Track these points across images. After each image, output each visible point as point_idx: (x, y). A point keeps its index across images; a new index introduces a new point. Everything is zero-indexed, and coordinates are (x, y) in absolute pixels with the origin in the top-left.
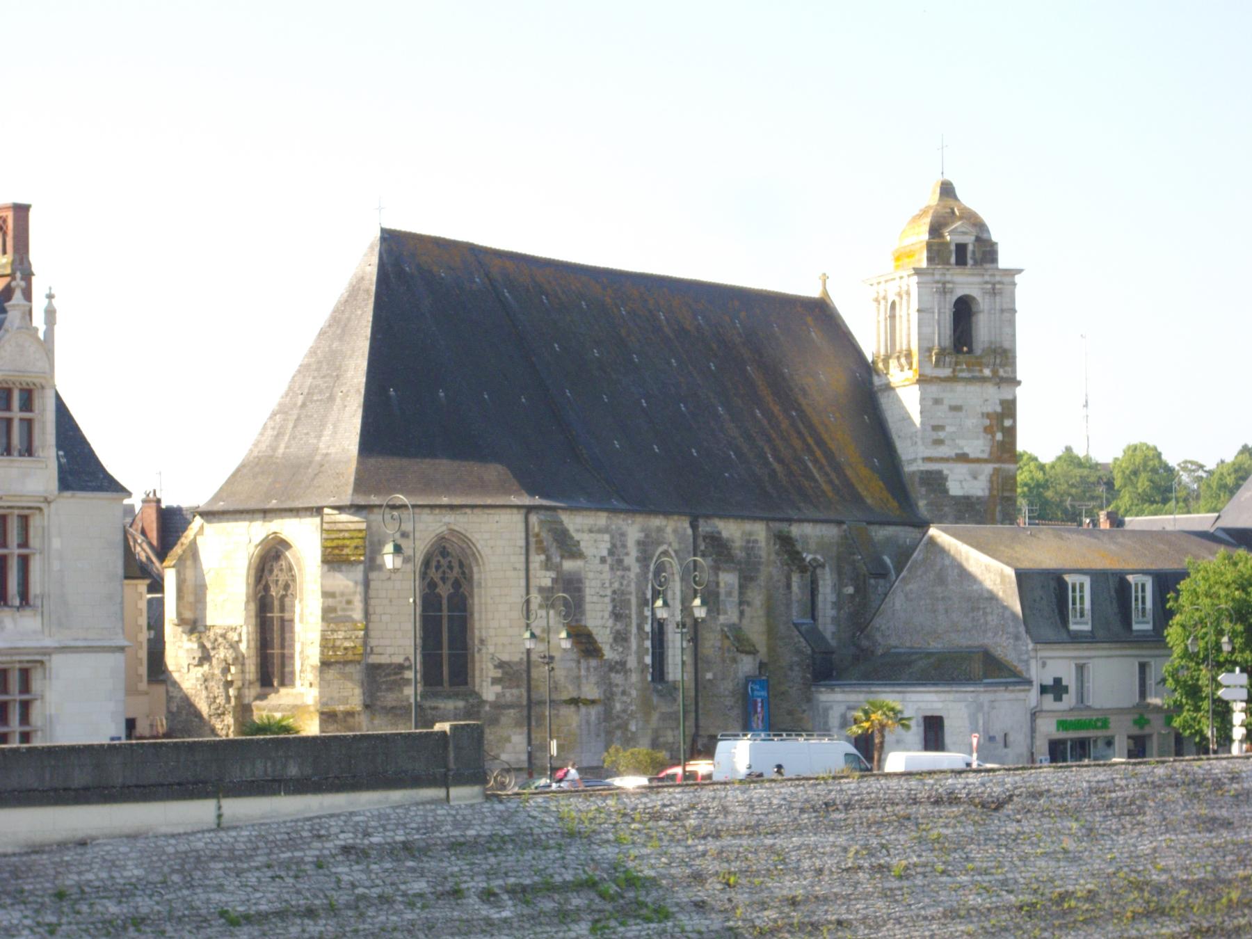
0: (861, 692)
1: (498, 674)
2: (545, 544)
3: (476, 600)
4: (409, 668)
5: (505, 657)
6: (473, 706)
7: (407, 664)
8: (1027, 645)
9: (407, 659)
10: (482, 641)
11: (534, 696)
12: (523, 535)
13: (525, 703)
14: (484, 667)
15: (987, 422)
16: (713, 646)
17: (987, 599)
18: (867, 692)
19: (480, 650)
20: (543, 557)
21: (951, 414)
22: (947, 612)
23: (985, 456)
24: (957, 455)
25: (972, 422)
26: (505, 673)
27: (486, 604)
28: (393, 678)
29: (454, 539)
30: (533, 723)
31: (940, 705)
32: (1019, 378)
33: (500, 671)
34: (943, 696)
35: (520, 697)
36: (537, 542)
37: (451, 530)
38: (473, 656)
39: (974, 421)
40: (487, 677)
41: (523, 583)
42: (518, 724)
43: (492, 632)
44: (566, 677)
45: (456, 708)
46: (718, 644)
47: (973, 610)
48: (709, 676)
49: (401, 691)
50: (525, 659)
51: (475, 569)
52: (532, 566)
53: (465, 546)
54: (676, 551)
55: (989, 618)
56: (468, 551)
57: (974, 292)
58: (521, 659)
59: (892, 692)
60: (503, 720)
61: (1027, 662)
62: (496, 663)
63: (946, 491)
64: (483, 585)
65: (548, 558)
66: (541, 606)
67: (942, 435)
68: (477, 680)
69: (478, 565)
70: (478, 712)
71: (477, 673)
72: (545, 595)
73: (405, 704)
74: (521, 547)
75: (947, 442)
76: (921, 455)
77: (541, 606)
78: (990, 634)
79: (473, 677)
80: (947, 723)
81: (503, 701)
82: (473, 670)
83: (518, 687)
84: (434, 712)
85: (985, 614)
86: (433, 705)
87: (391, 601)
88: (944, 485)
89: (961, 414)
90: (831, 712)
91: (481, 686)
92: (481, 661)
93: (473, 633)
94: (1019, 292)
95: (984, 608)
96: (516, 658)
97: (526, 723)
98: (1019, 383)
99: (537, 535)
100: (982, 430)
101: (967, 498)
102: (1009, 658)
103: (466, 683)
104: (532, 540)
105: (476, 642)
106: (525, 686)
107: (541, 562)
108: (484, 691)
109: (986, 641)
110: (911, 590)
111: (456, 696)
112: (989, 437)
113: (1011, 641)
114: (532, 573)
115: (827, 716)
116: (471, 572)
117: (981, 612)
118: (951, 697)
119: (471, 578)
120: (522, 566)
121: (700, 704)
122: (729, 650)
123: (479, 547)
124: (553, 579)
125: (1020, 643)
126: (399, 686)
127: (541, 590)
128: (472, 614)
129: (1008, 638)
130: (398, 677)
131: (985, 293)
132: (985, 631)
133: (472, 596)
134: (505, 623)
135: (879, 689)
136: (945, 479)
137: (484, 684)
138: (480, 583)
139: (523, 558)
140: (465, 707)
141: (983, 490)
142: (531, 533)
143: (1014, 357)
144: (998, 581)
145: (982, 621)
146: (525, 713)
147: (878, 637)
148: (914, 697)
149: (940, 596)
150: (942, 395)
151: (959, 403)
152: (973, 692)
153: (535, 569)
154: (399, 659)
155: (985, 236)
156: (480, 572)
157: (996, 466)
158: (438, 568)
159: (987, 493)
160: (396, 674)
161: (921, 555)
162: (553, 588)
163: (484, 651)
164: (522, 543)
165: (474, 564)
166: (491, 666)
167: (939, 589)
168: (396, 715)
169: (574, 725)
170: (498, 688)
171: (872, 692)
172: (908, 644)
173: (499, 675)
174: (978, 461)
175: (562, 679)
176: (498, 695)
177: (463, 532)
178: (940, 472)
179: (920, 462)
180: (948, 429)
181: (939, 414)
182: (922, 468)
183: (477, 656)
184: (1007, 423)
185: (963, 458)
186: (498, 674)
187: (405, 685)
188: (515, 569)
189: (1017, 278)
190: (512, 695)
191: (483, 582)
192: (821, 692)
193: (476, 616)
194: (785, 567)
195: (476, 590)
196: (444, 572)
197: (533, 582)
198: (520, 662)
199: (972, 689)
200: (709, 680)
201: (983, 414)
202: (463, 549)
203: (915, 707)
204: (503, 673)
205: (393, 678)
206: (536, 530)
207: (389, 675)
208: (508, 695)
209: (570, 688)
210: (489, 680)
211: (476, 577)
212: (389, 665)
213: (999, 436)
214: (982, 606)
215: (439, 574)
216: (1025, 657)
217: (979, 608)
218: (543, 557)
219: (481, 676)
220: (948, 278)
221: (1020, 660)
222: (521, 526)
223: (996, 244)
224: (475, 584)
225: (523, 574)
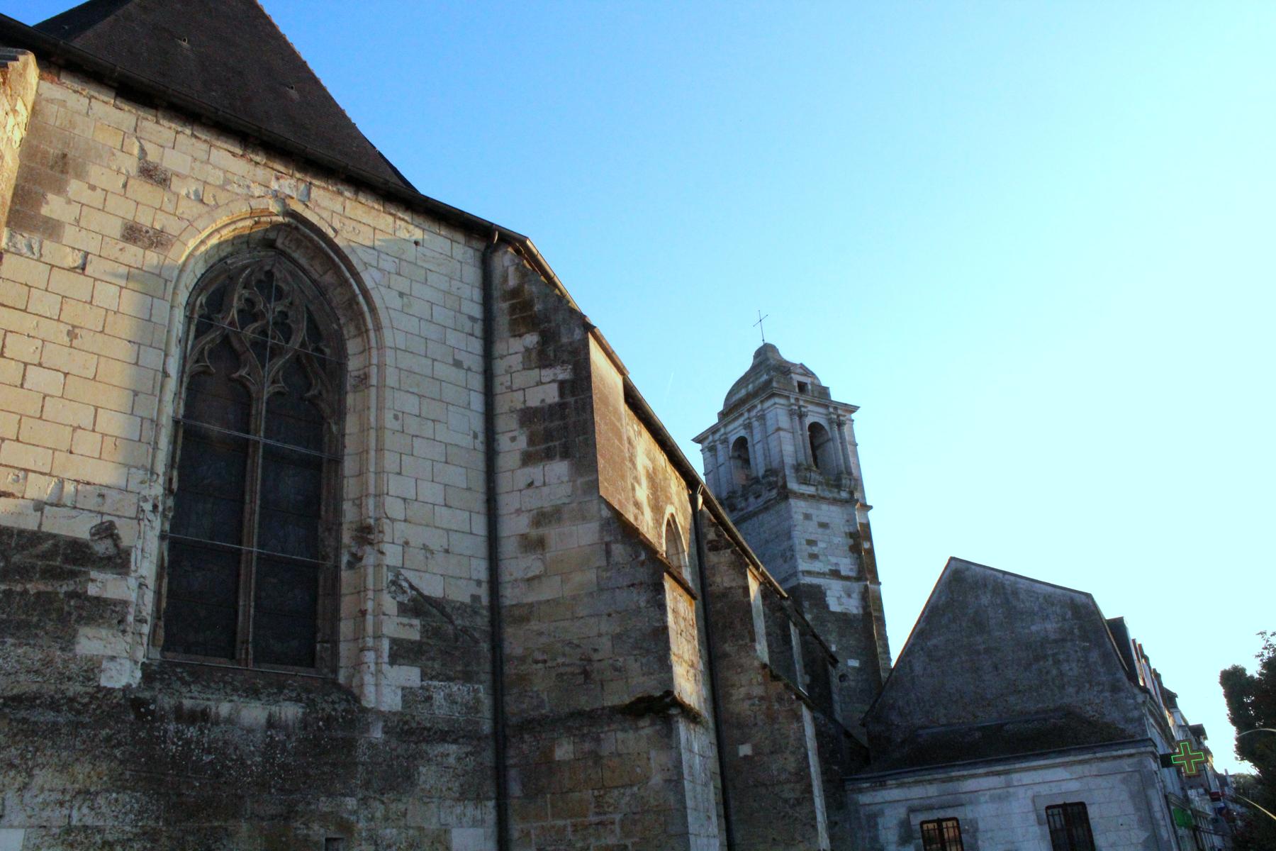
0: (930, 782)
1: (412, 631)
2: (538, 307)
3: (351, 424)
4: (119, 562)
5: (432, 587)
6: (329, 720)
7: (102, 547)
8: (1134, 697)
9: (107, 531)
10: (365, 534)
11: (515, 706)
12: (477, 294)
13: (487, 727)
14: (370, 606)
15: (851, 542)
16: (749, 697)
17: (1056, 641)
18: (943, 781)
19: (356, 560)
20: (531, 339)
21: (820, 530)
22: (996, 668)
23: (853, 574)
24: (830, 570)
25: (841, 541)
26: (431, 632)
27: (380, 429)
28: (32, 588)
29: (296, 255)
30: (515, 789)
31: (1074, 786)
32: (869, 503)
33: (416, 622)
34: (1079, 769)
35: (474, 708)
36: (513, 309)
37: (293, 215)
38: (336, 579)
39: (840, 539)
40: (378, 637)
41: (477, 402)
42: (468, 794)
43: (394, 508)
44: (616, 638)
45: (271, 723)
46: (758, 691)
47: (1037, 659)
48: (745, 750)
49: (68, 643)
50: (485, 601)
51: (352, 346)
52: (500, 366)
53: (329, 278)
54: (682, 526)
55: (1065, 667)
56: (337, 297)
57: (823, 422)
58: (475, 598)
59: (987, 774)
60: (427, 775)
61: (1140, 720)
62: (405, 599)
63: (827, 607)
64: (374, 381)
65: (548, 338)
66: (528, 459)
67: (815, 550)
68: (344, 648)
69: (362, 331)
70: (350, 745)
71: (346, 628)
72: (539, 427)
73: (74, 688)
74: (472, 318)
75: (820, 557)
77: (528, 459)
78: (1071, 690)
79: (335, 643)
80: (1093, 812)
81: (422, 714)
82: (335, 618)
83: (468, 677)
84: (192, 732)
85: (1057, 662)
86: (187, 703)
87: (72, 334)
88: (825, 601)
90: (880, 821)
91: (358, 665)
92: (360, 591)
93: (338, 512)
94: (856, 426)
95: (1054, 655)
96: (461, 593)
97: (489, 788)
98: (871, 507)
99: (515, 293)
100: (847, 548)
101: (845, 614)
102: (1108, 719)
103: (309, 659)
104: (501, 307)
105: (346, 538)
106: (487, 677)
107: (528, 350)
108: (369, 679)
109: (1067, 700)
110: (936, 646)
111: (278, 689)
113: (1107, 694)
114: (501, 381)
115: (876, 824)
116: (342, 353)
117: (1050, 662)
118: (1094, 768)
119: (341, 366)
120: (476, 363)
121: (733, 803)
122: (780, 699)
123: (369, 284)
124: (562, 384)
125: (1122, 694)
126: (63, 619)
127: (528, 416)
128: (337, 461)
129: (1102, 691)
130: (65, 587)
131: (831, 422)
132: (1062, 687)
133: (340, 414)
134: (431, 492)
135: (965, 773)
136: (825, 594)
137: (370, 657)
138: (364, 379)
139: (477, 346)
140: (305, 724)
141: (857, 608)
142: (496, 294)
143: (862, 485)
144: (1069, 614)
145: (1054, 672)
146: (488, 757)
147: (895, 718)
148: (1027, 778)
149: (982, 647)
150: (810, 511)
151: (825, 520)
152: (1131, 756)
153: (509, 371)
154: (80, 528)
155: (816, 382)
156: (366, 350)
158: (249, 314)
159: (861, 611)
160: (52, 574)
161: (943, 598)
162: (562, 406)
163: (370, 558)
164: (477, 311)
165: (349, 331)
166: (389, 604)
167: (979, 639)
168: (29, 731)
169: (657, 779)
170: (410, 675)
171: (951, 780)
172: (943, 721)
173: (415, 636)
174: (847, 578)
175: (606, 644)
176: (407, 693)
177: (331, 233)
178: (819, 587)
180: (822, 545)
181: (810, 530)
183: (345, 575)
184: (866, 545)
185: (835, 574)
186: (412, 631)
187: (90, 620)
188: (458, 364)
189: (853, 416)
190: (450, 698)
191: (374, 370)
192: (861, 791)
193: (349, 466)
194: (778, 614)
195: (350, 399)
196: (264, 333)
197: (504, 403)
198: (471, 609)
199: (1133, 751)
200: (746, 757)
201: (846, 533)
202: (322, 291)
203: (1030, 793)
204: (424, 631)
205: (32, 588)
206: (512, 282)
207: (24, 573)
208: (439, 697)
209: (633, 666)
210: (386, 645)
211: (353, 364)
212: (36, 537)
214: (1050, 652)
215: (250, 331)
216: (1136, 714)
217: (1045, 657)
218: (531, 339)
219: (359, 635)
220: (801, 403)
221: (1131, 720)
222: (472, 273)
223: (828, 388)
224: (350, 382)
225: (477, 382)
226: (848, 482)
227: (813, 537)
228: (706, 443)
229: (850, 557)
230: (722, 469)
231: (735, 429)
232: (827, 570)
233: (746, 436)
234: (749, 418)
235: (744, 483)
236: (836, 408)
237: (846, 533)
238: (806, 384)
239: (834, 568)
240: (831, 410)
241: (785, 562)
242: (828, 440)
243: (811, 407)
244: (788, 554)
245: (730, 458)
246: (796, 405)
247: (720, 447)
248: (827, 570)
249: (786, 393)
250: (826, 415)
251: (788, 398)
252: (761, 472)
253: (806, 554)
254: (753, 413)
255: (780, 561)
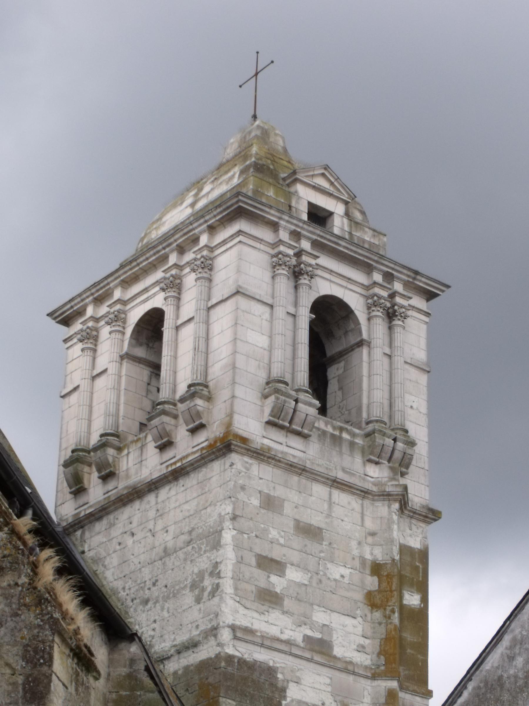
21: (297, 542)
23: (360, 658)
24: (307, 639)
39: (346, 572)
75: (287, 603)
76: (229, 620)
89: (313, 547)
100: (359, 596)
112: (378, 615)
150: (279, 492)
157: (394, 684)
178: (271, 671)
179: (226, 635)
181: (273, 533)
182: (230, 651)
213: (396, 618)
220: (306, 245)
226: (389, 442)
227: (276, 554)
228: (77, 326)
229: (364, 617)
230: (100, 382)
231: (146, 290)
232: (298, 637)
233: (164, 308)
234: (176, 265)
235: (147, 417)
236: (389, 277)
237: (363, 561)
238: (331, 214)
239: (318, 635)
240: (378, 277)
241: (198, 600)
242: (360, 344)
243: (325, 261)
244: (208, 583)
245: (122, 357)
246: (290, 247)
247: (105, 331)
248: (298, 637)
249: (272, 215)
250: (368, 288)
251: (274, 226)
252: (182, 389)
253: (251, 588)
254: (189, 256)
255: (188, 598)
